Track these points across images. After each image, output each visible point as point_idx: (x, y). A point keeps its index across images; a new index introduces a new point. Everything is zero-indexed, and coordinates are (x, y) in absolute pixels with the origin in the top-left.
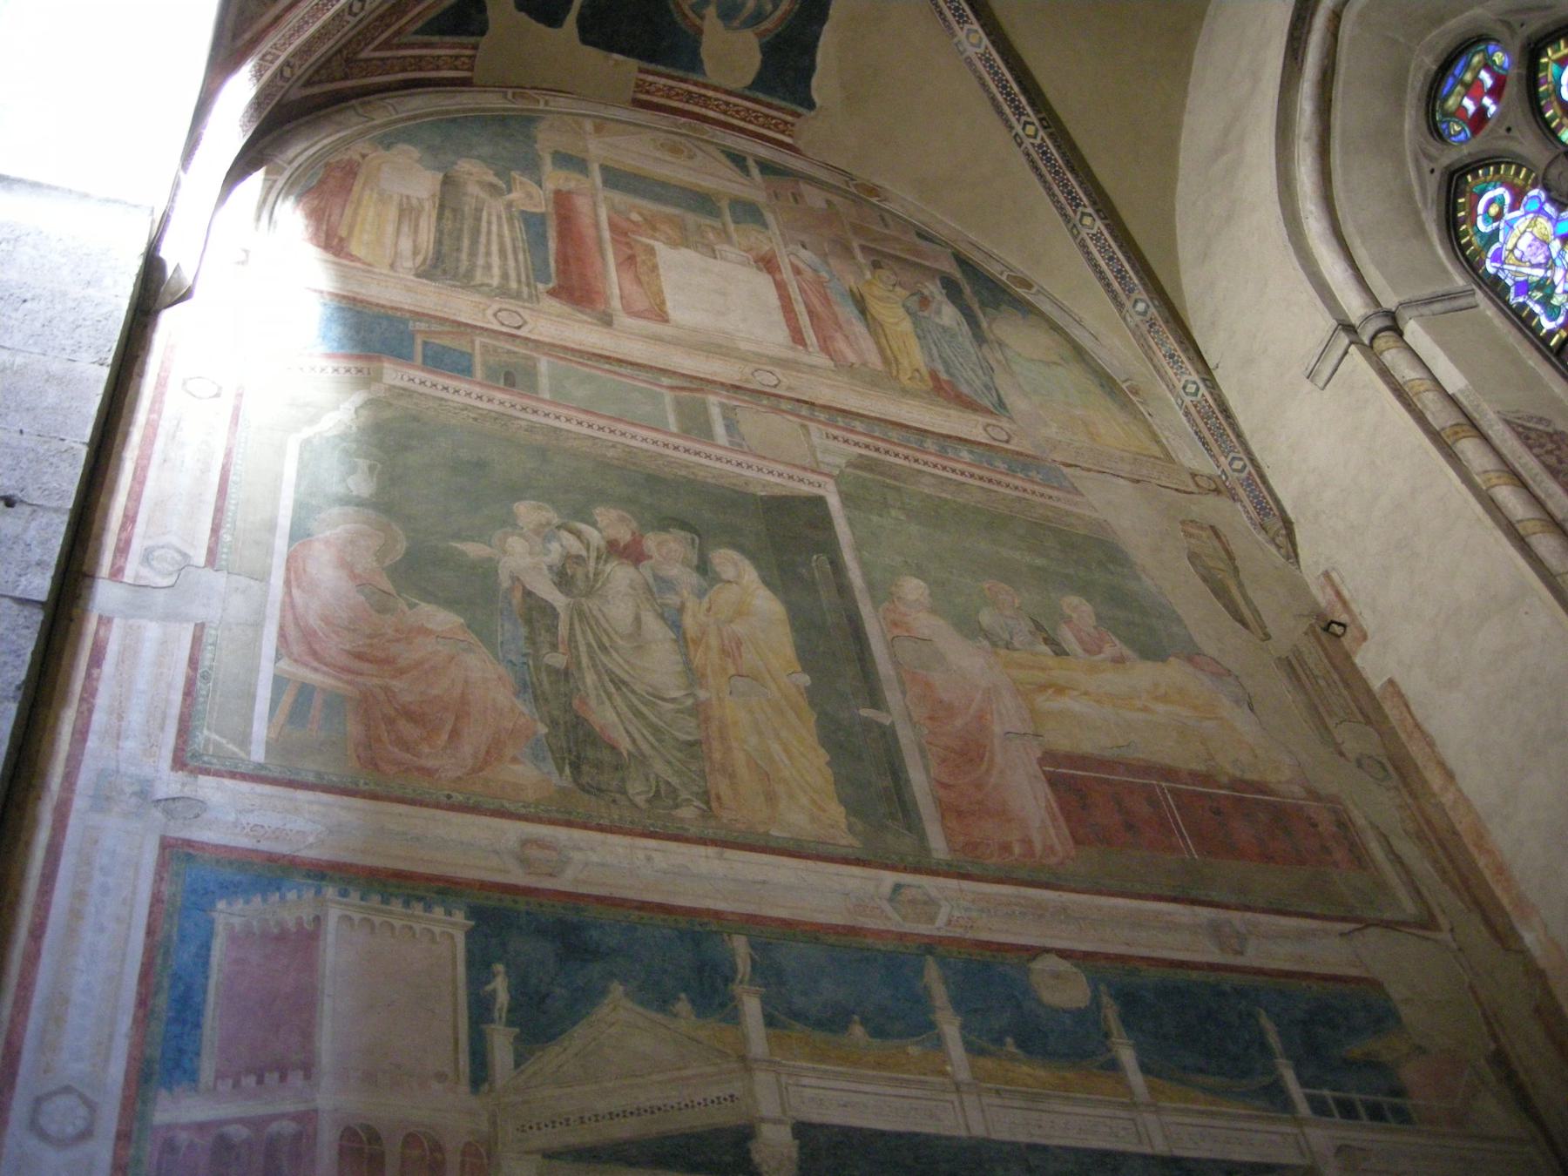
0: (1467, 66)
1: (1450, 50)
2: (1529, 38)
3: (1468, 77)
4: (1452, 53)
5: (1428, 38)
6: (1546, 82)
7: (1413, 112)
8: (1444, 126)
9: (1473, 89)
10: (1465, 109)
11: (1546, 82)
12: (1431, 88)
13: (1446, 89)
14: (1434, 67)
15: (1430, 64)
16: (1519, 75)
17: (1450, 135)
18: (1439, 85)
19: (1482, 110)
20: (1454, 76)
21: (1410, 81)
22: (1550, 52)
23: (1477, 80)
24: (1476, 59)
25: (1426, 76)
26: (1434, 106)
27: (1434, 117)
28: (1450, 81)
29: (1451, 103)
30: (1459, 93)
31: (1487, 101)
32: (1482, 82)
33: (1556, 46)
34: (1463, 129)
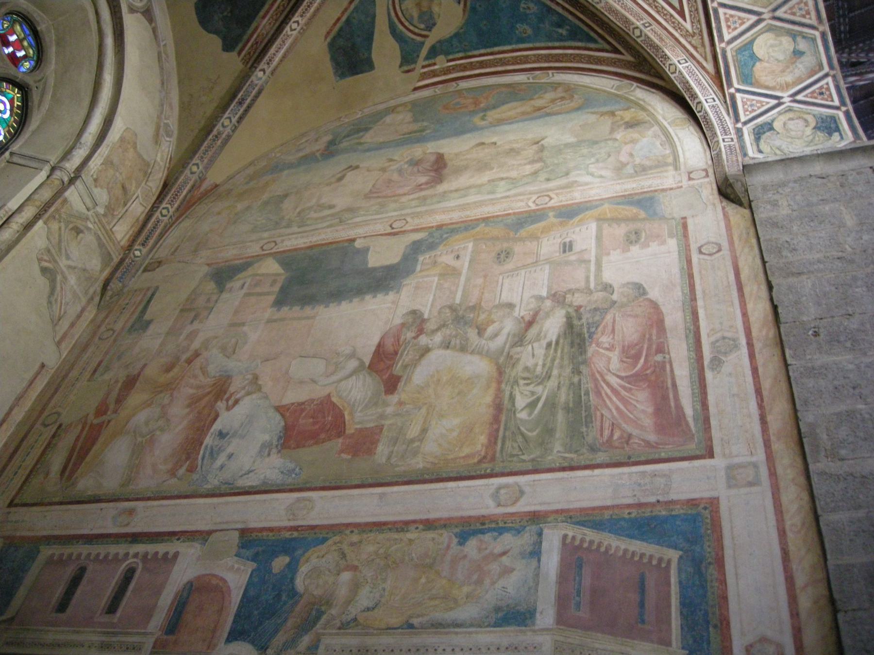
0: (30, 45)
1: (42, 41)
2: (31, 90)
3: (25, 44)
4: (40, 39)
5: (53, 31)
6: (7, 88)
7: (25, 6)
8: (9, 18)
9: (18, 45)
10: (12, 35)
11: (7, 88)
12: (30, 20)
13: (24, 27)
14: (39, 29)
15: (41, 28)
16: (18, 78)
17: (4, 20)
18: (29, 26)
19: (7, 44)
20: (29, 35)
21: (39, 12)
22: (18, 95)
23: (23, 48)
24: (31, 52)
25: (37, 22)
26: (22, 18)
27: (16, 15)
28: (28, 32)
29: (18, 28)
30: (20, 35)
31: (11, 49)
32: (20, 50)
33: (20, 100)
34: (4, 29)
